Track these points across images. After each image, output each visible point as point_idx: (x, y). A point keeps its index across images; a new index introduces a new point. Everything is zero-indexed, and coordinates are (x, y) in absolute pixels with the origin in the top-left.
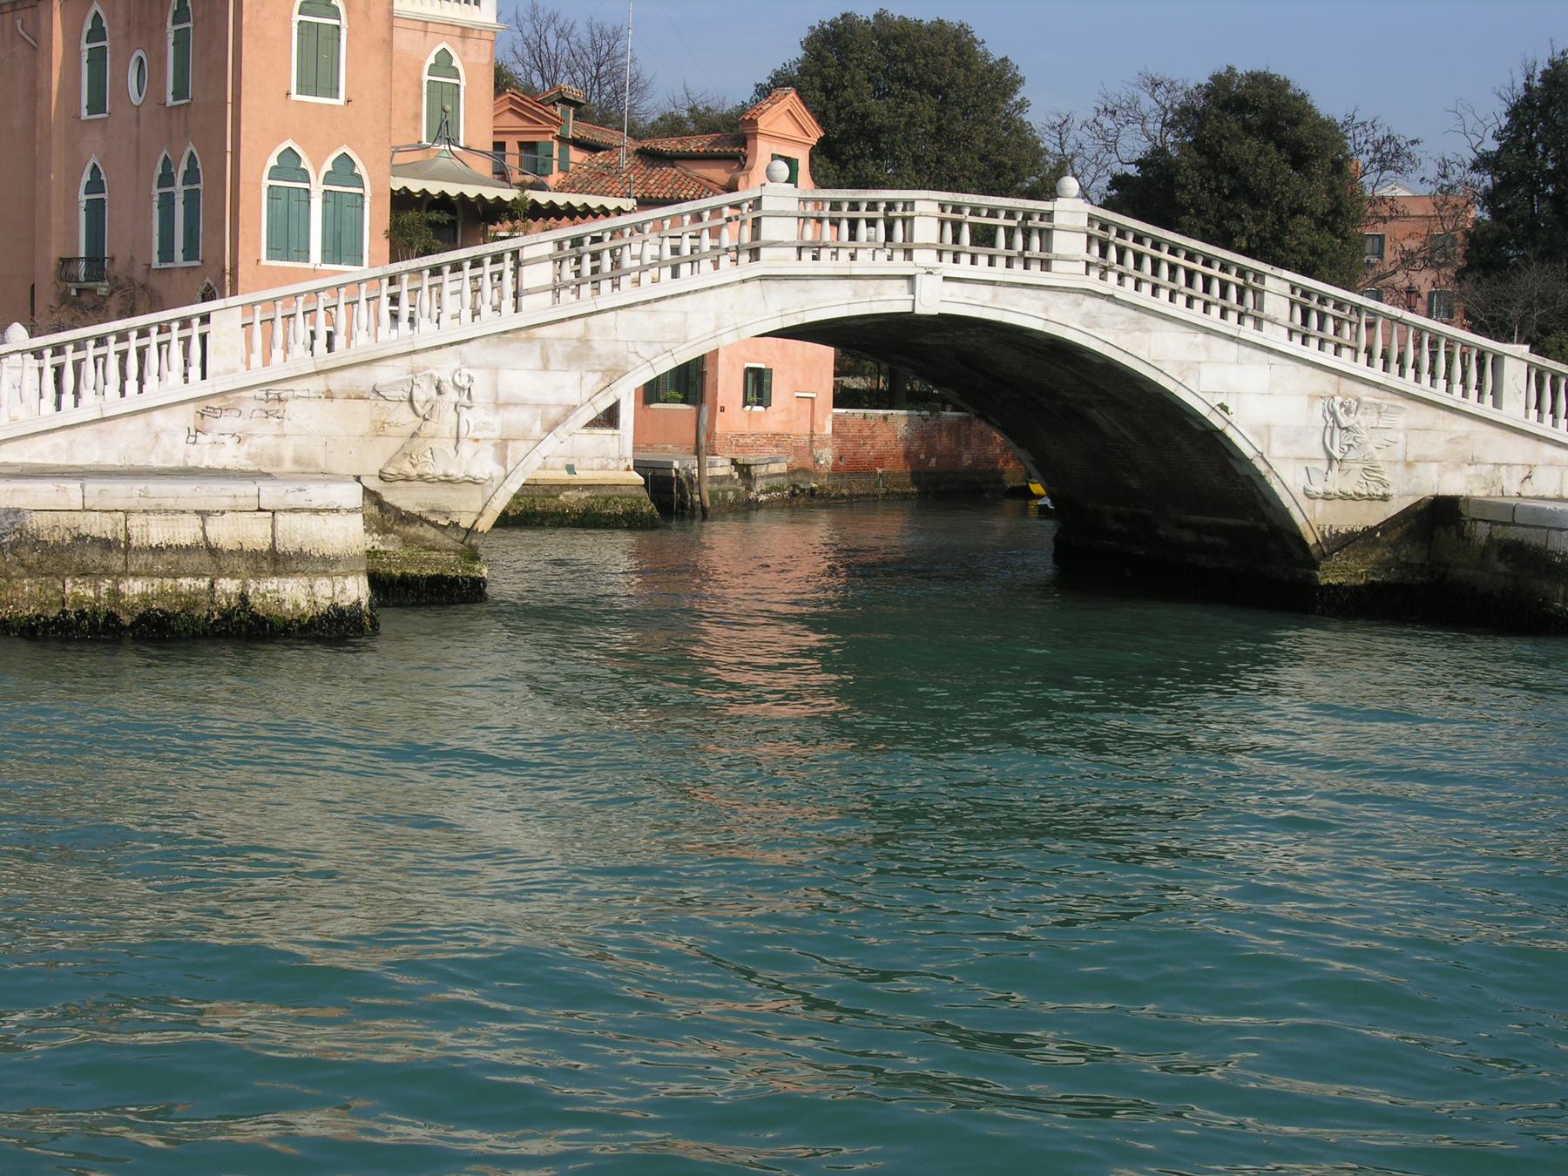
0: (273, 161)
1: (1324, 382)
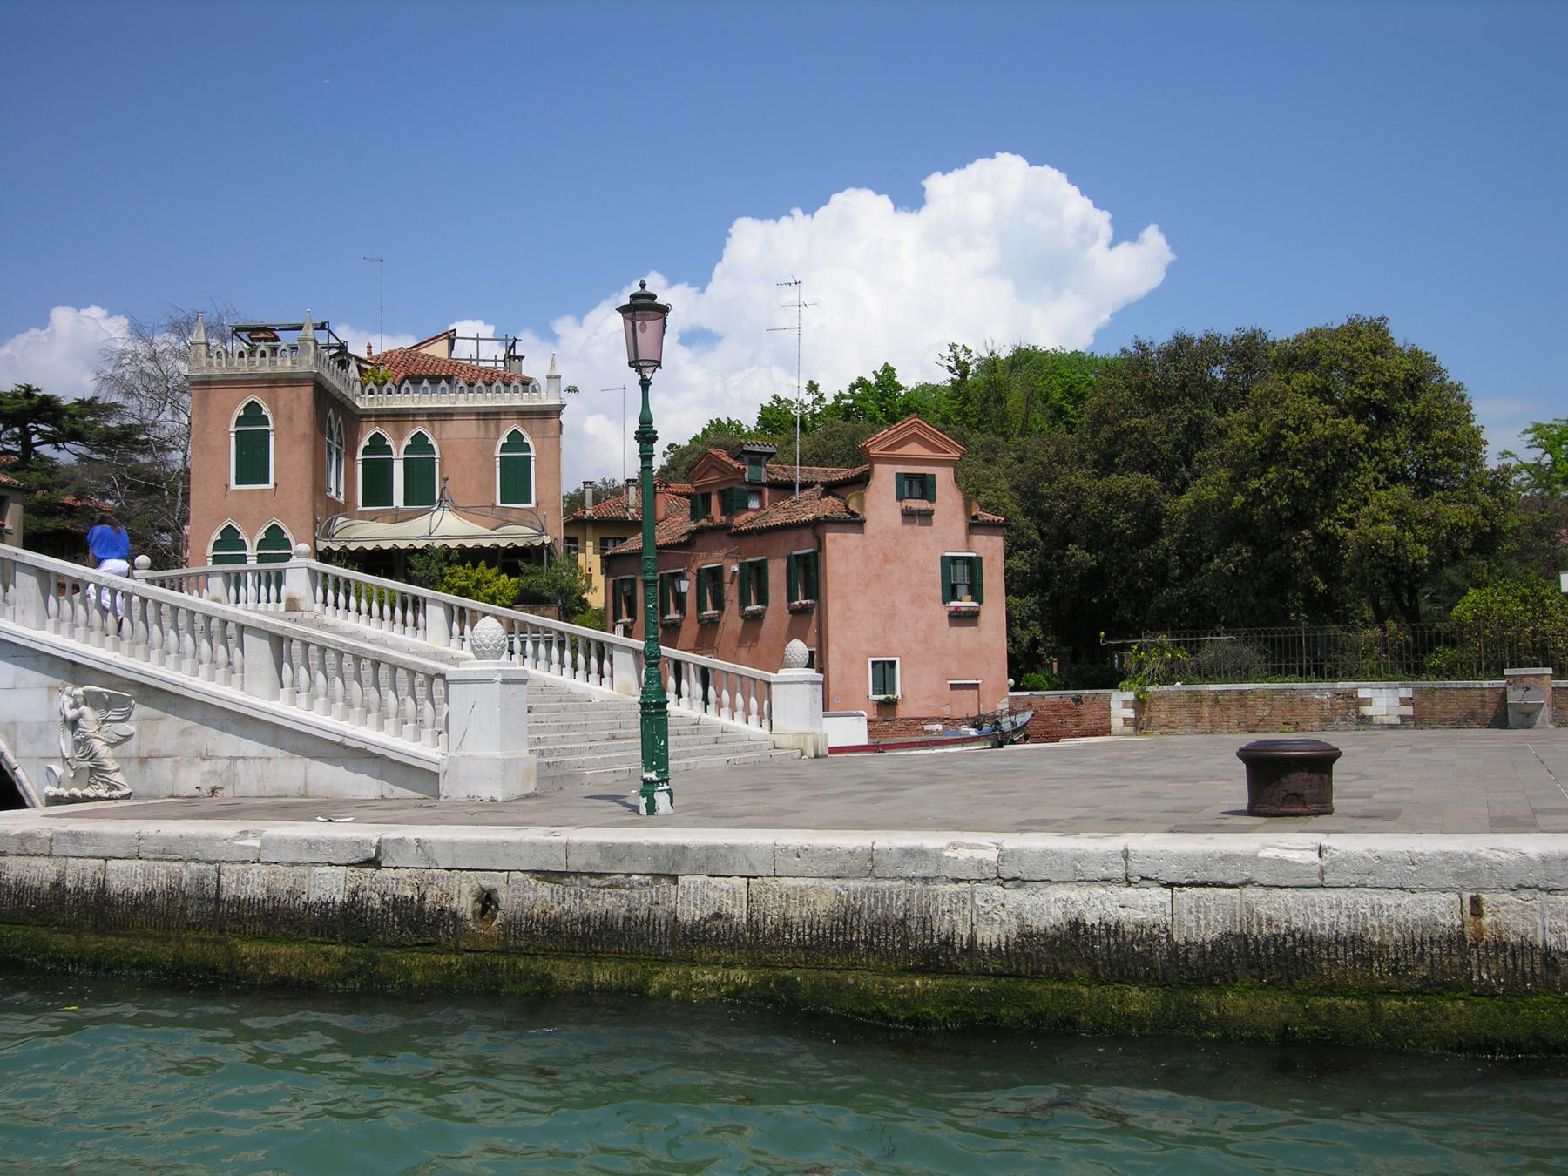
0: (216, 536)
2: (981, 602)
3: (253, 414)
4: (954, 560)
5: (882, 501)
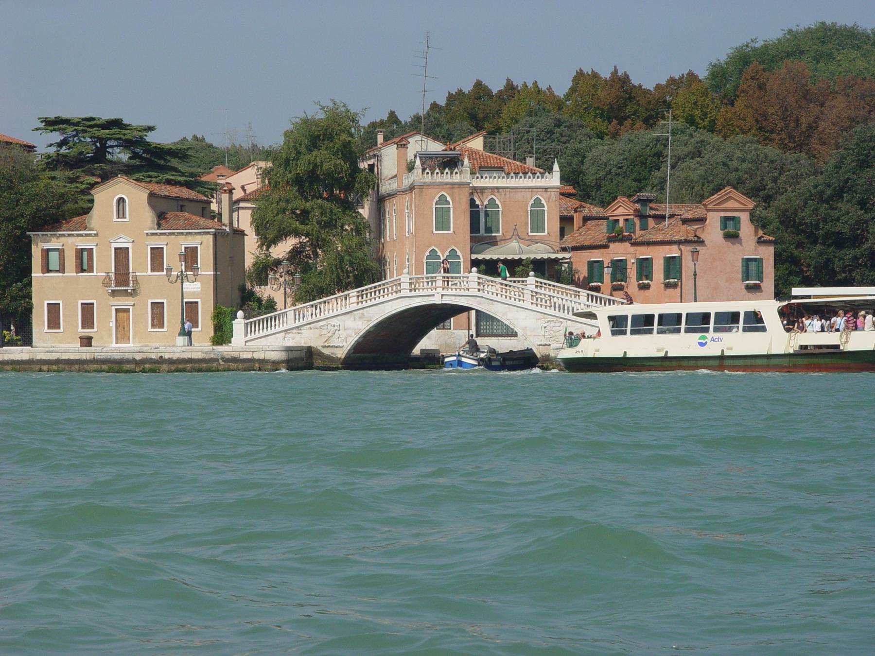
0: (427, 253)
2: (762, 281)
3: (442, 200)
4: (748, 260)
5: (713, 232)
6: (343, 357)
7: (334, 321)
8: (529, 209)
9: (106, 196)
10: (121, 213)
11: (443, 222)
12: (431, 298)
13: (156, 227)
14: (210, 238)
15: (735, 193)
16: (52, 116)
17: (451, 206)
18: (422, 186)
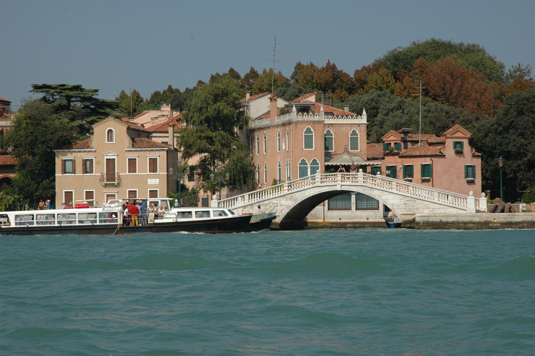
0: (300, 162)
1: (402, 197)
2: (475, 178)
3: (308, 131)
4: (468, 166)
5: (449, 150)
6: (279, 222)
7: (274, 201)
8: (350, 136)
9: (101, 129)
10: (110, 139)
11: (309, 144)
12: (334, 187)
13: (132, 146)
14: (165, 153)
15: (461, 129)
16: (40, 83)
17: (313, 134)
18: (297, 123)
